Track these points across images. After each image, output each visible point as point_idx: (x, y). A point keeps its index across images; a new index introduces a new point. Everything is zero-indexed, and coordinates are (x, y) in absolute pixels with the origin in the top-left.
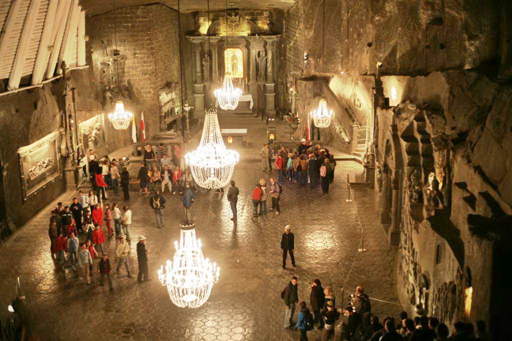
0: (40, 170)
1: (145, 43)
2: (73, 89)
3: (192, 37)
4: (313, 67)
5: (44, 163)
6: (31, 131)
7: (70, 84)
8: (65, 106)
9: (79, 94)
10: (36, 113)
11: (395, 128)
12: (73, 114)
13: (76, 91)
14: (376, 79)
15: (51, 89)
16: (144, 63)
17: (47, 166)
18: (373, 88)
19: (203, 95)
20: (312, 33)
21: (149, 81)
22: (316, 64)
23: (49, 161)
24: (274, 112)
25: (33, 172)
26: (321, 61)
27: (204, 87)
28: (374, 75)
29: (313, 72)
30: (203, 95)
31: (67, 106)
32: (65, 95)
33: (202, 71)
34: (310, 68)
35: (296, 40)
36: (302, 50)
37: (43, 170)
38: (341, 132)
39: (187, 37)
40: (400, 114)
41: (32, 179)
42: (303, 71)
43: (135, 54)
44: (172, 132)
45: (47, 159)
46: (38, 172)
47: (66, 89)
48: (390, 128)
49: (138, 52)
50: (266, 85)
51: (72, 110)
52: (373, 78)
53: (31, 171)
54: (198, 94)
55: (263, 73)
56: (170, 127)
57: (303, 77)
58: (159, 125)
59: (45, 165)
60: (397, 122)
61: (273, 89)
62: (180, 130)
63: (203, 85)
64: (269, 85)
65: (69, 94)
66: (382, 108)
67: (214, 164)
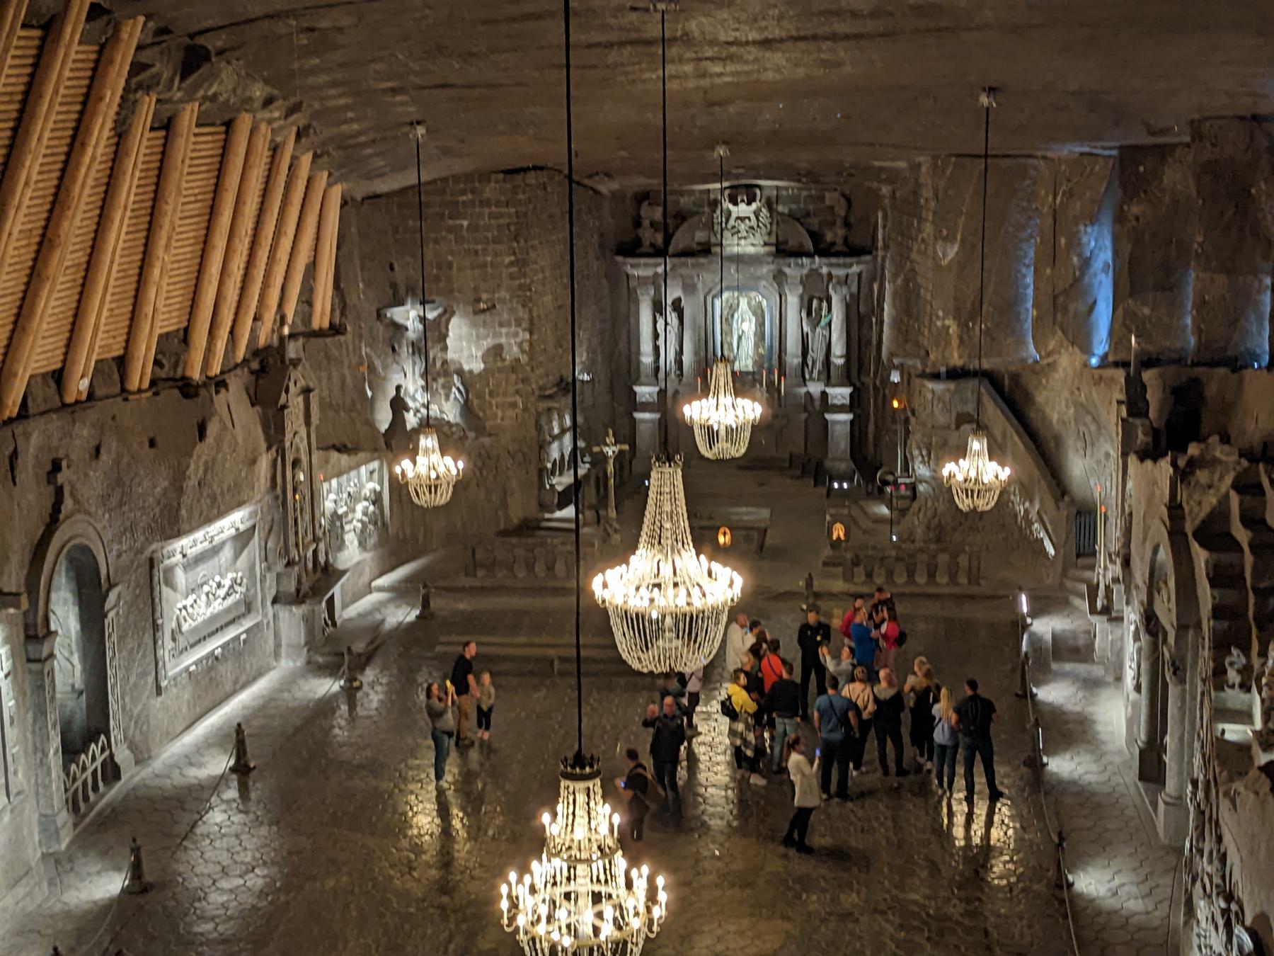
0: (208, 604)
1: (505, 272)
2: (306, 391)
3: (630, 260)
4: (955, 342)
5: (219, 585)
6: (187, 500)
7: (298, 378)
8: (284, 434)
9: (325, 406)
10: (203, 451)
11: (1175, 510)
12: (304, 459)
13: (314, 397)
14: (1127, 378)
15: (247, 389)
16: (501, 325)
17: (228, 594)
18: (1119, 402)
19: (656, 416)
20: (952, 251)
21: (514, 376)
23: (234, 581)
24: (845, 465)
25: (190, 610)
28: (1125, 365)
29: (956, 360)
30: (656, 416)
31: (288, 436)
32: (284, 407)
35: (913, 270)
36: (929, 298)
37: (217, 606)
38: (1030, 524)
39: (620, 259)
40: (1192, 473)
41: (185, 627)
42: (928, 353)
43: (478, 300)
45: (230, 575)
46: (201, 611)
47: (287, 391)
48: (1164, 511)
49: (484, 296)
50: (829, 390)
51: (303, 446)
52: (1120, 375)
53: (185, 608)
54: (643, 410)
55: (820, 357)
56: (565, 499)
57: (928, 370)
58: (536, 492)
59: (222, 592)
60: (1183, 495)
61: (847, 402)
62: (591, 507)
63: (656, 389)
65: (295, 403)
66: (1143, 456)
67: (672, 601)
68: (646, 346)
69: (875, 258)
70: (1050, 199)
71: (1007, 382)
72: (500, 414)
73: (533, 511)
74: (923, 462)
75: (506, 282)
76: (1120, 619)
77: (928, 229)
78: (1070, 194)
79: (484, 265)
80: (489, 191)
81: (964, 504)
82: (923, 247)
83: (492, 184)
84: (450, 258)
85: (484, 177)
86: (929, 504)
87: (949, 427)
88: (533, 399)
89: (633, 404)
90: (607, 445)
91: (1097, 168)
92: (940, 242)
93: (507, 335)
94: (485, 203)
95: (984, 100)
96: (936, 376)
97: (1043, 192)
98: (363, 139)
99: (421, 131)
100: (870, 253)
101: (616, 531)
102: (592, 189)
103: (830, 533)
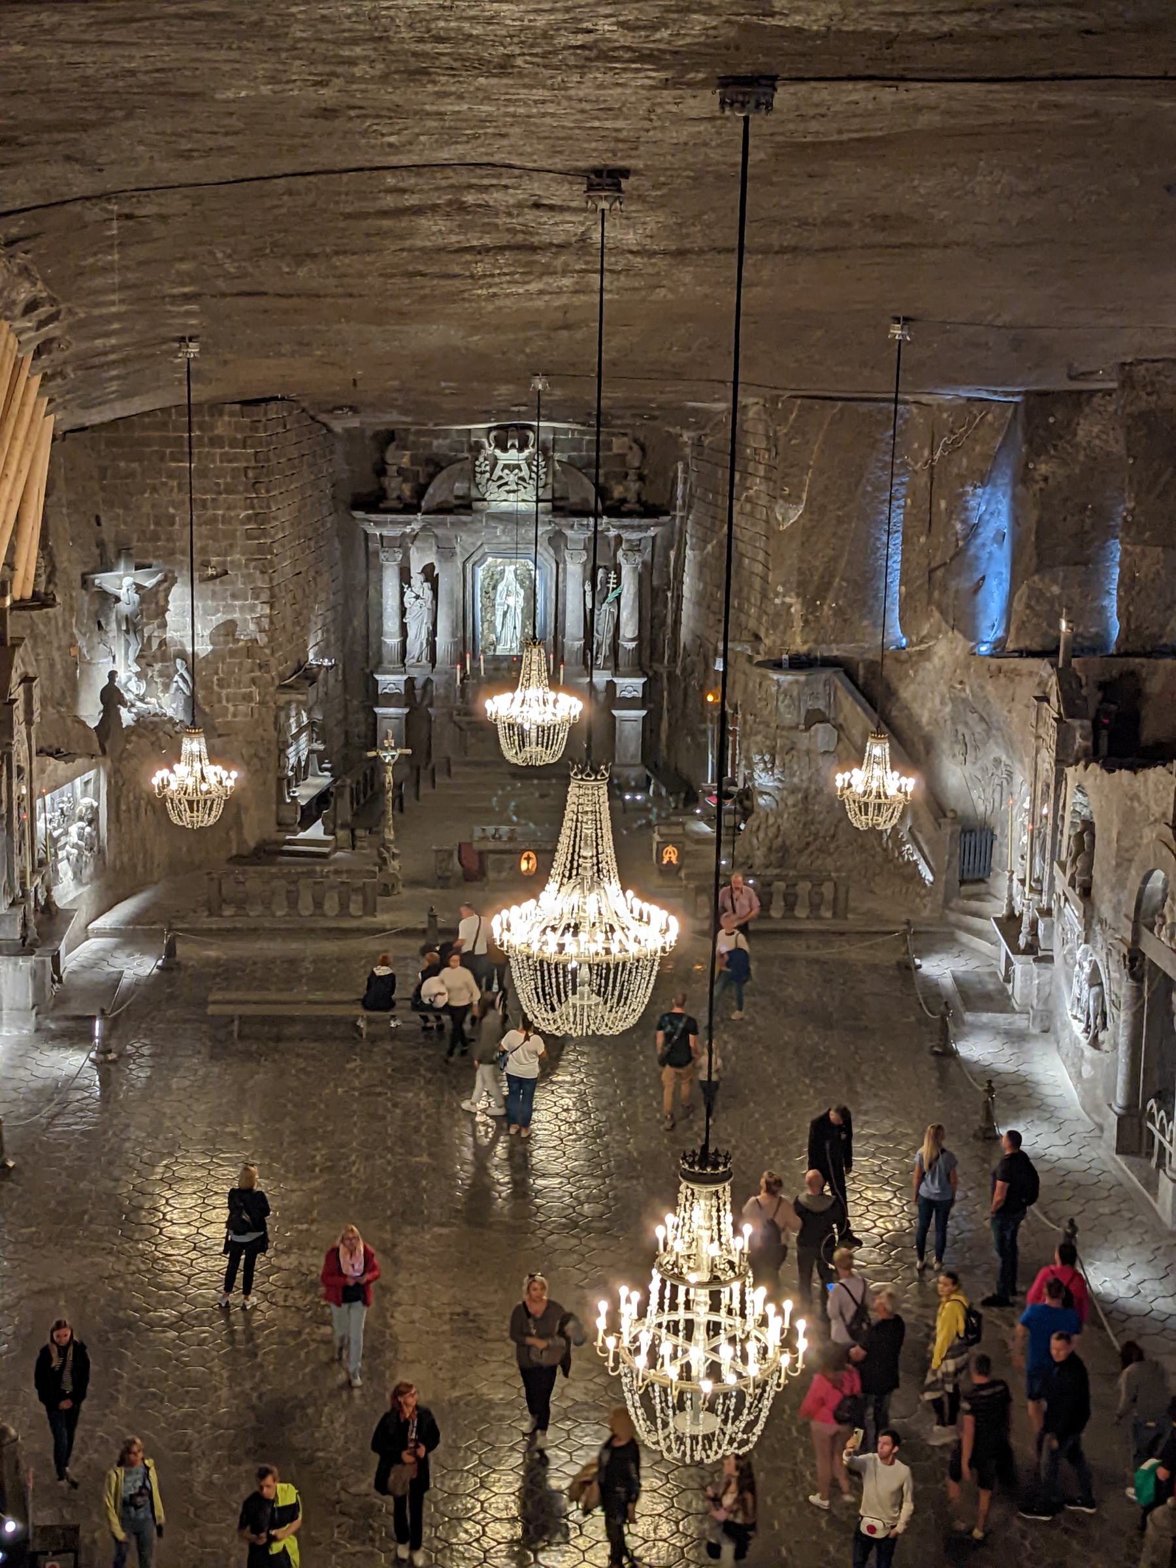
3: (373, 517)
4: (798, 624)
16: (234, 596)
19: (406, 710)
20: (796, 514)
22: (811, 617)
26: (825, 607)
27: (410, 682)
29: (799, 644)
30: (406, 710)
33: (404, 628)
34: (789, 625)
39: (359, 514)
42: (757, 637)
44: (316, 831)
49: (214, 559)
52: (1043, 668)
56: (308, 816)
57: (759, 658)
58: (274, 807)
62: (344, 826)
64: (628, 681)
68: (391, 625)
69: (674, 517)
70: (926, 453)
71: (861, 672)
72: (231, 709)
73: (270, 831)
74: (765, 770)
75: (241, 541)
76: (1049, 959)
77: (757, 486)
78: (954, 448)
79: (213, 520)
80: (222, 426)
81: (860, 822)
82: (748, 507)
83: (226, 418)
84: (171, 510)
85: (216, 407)
86: (771, 820)
87: (796, 727)
88: (272, 689)
89: (373, 696)
90: (386, 749)
91: (990, 417)
92: (781, 502)
93: (242, 608)
94: (215, 442)
95: (897, 331)
96: (777, 665)
97: (916, 446)
98: (112, 357)
99: (193, 349)
100: (667, 513)
101: (394, 856)
102: (325, 425)
103: (660, 857)
